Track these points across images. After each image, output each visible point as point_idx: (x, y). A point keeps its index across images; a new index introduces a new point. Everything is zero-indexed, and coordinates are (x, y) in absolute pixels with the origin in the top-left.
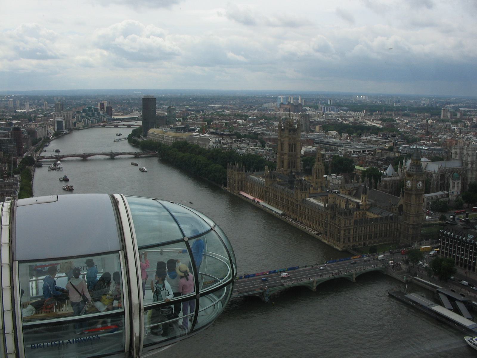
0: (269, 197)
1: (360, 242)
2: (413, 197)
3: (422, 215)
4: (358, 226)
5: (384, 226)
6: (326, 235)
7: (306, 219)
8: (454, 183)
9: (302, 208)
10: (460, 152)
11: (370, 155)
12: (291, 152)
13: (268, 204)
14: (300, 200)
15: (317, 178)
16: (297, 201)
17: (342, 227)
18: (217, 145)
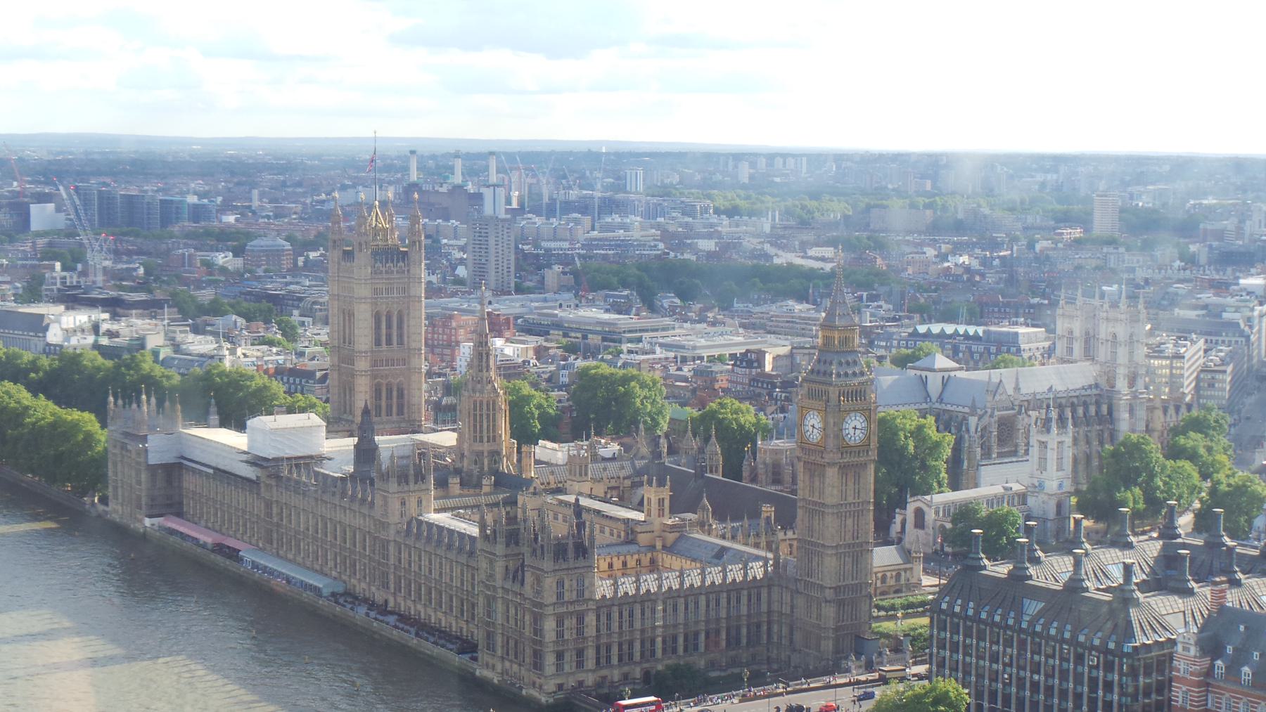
0: (278, 525)
1: (626, 669)
2: (832, 474)
3: (905, 570)
4: (616, 603)
5: (724, 602)
6: (491, 647)
7: (420, 599)
8: (1046, 447)
9: (404, 555)
10: (1087, 333)
11: (744, 363)
12: (384, 347)
13: (278, 555)
14: (396, 524)
15: (475, 441)
16: (384, 526)
17: (546, 606)
18: (83, 342)
